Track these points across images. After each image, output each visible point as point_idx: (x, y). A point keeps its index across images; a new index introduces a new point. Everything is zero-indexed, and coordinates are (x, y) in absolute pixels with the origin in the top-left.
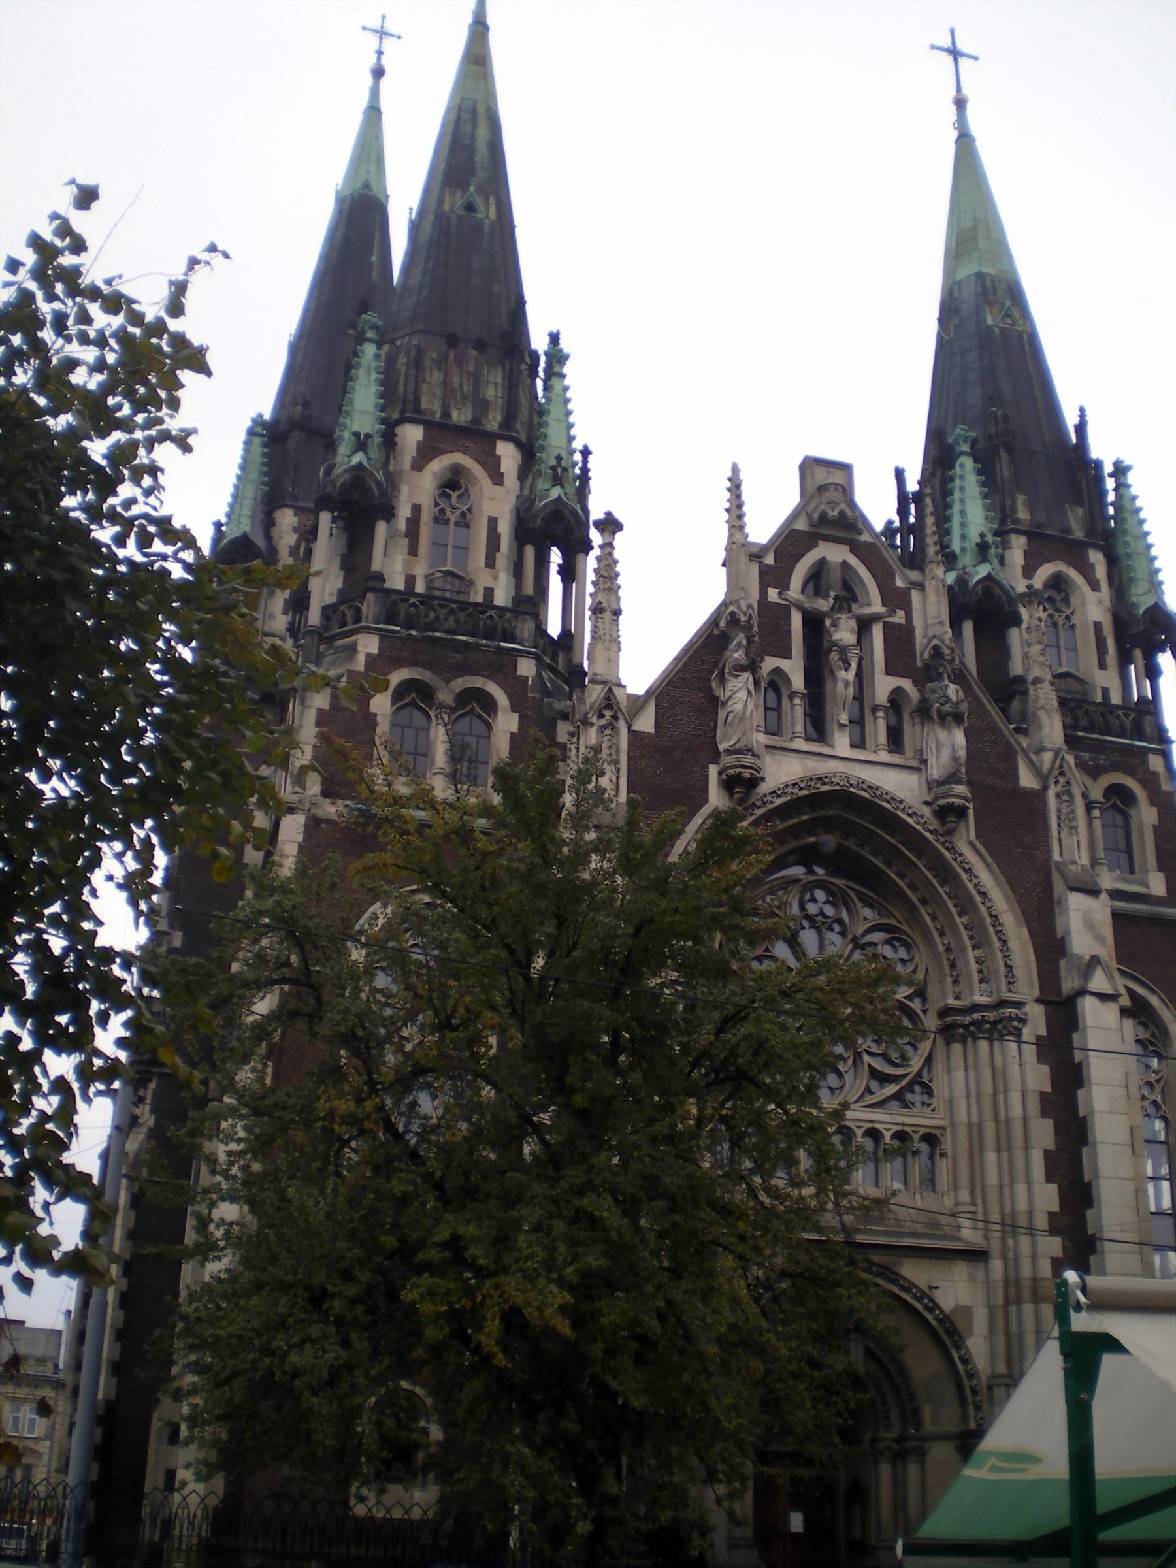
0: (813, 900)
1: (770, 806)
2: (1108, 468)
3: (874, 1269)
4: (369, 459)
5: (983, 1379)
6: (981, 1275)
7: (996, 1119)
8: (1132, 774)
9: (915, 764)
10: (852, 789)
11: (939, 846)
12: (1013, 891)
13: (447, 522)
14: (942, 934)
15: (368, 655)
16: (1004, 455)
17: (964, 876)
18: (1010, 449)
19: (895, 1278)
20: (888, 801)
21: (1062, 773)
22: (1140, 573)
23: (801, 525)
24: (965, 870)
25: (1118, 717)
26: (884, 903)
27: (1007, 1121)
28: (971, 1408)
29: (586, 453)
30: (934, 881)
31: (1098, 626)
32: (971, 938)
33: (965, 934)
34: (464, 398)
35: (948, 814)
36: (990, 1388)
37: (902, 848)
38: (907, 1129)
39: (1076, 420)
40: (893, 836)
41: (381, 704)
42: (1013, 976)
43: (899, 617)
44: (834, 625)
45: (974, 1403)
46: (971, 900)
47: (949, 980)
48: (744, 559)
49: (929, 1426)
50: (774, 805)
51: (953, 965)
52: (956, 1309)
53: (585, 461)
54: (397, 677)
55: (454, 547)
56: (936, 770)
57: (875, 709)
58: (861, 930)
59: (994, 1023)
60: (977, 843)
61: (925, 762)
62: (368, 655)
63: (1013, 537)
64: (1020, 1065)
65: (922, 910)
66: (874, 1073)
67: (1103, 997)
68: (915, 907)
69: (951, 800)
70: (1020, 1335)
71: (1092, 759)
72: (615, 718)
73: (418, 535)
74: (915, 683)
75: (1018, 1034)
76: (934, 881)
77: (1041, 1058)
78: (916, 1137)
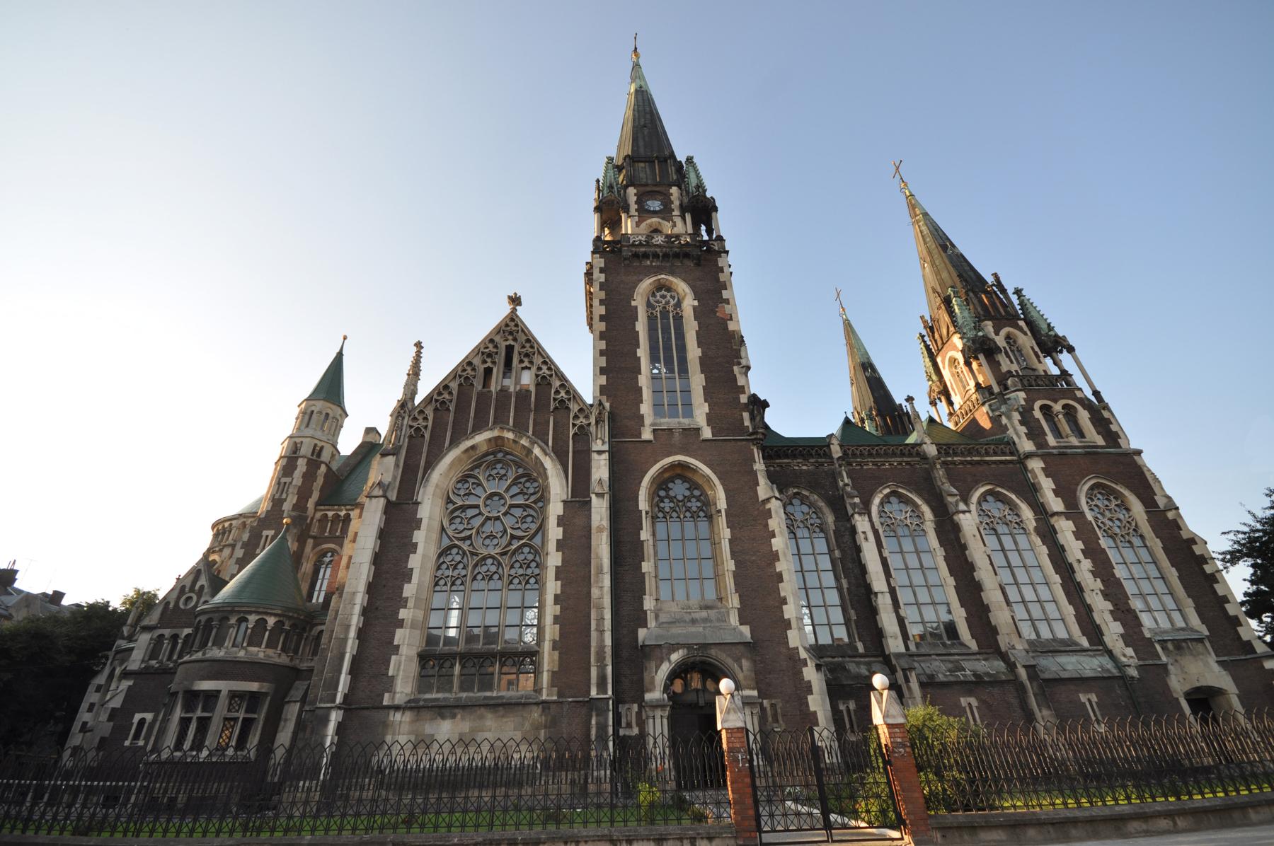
66: (513, 537)
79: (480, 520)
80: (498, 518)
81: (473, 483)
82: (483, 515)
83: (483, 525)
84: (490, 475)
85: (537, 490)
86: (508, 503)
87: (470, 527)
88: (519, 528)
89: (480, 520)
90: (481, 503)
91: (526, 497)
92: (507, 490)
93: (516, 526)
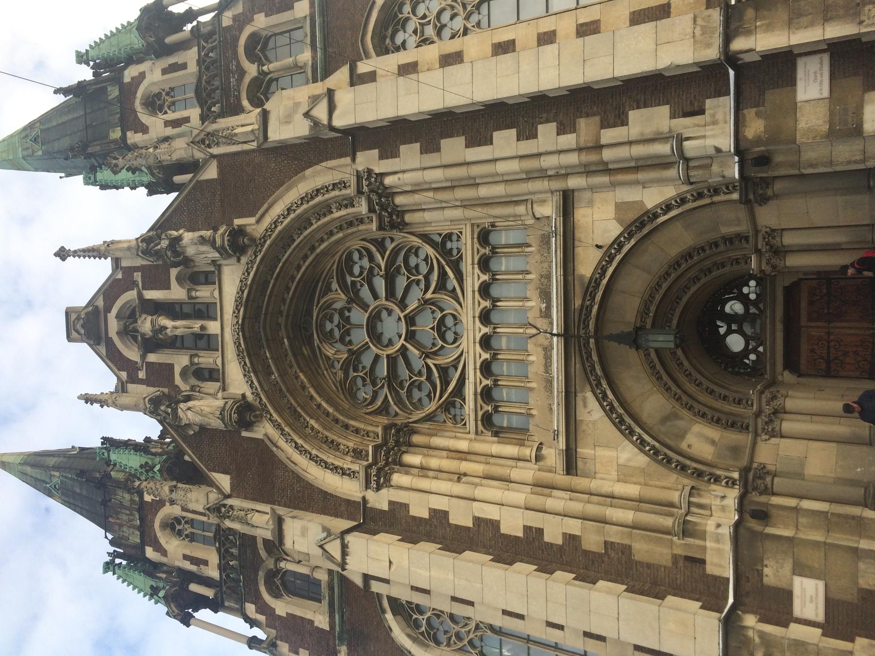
0: (332, 330)
1: (259, 390)
3: (588, 303)
4: (164, 588)
5: (686, 188)
6: (587, 195)
7: (452, 188)
8: (236, 39)
10: (240, 322)
11: (264, 249)
12: (283, 183)
13: (193, 533)
14: (331, 234)
17: (280, 228)
19: (594, 282)
20: (243, 292)
21: (203, 141)
23: (103, 349)
24: (276, 227)
25: (207, 55)
26: (325, 272)
27: (447, 180)
28: (716, 199)
30: (293, 247)
31: (165, 72)
32: (325, 215)
33: (324, 220)
34: (131, 514)
36: (691, 184)
37: (275, 274)
38: (476, 261)
40: (270, 282)
41: (282, 607)
42: (340, 183)
43: (138, 276)
45: (711, 196)
46: (299, 217)
47: (362, 227)
48: (124, 399)
49: (743, 227)
50: (258, 387)
51: (351, 224)
52: (619, 221)
55: (204, 531)
57: (190, 297)
58: (343, 296)
59: (380, 196)
60: (258, 216)
62: (257, 612)
63: (129, 142)
64: (404, 172)
65: (318, 251)
66: (442, 286)
67: (332, 108)
68: (318, 255)
69: (228, 248)
70: (637, 159)
71: (234, 77)
72: (224, 506)
73: (197, 559)
75: (382, 175)
76: (293, 247)
77: (395, 154)
78: (483, 251)
79: (413, 351)
80: (410, 320)
81: (355, 370)
82: (403, 350)
83: (418, 345)
84: (342, 340)
85: (365, 253)
86: (384, 302)
87: (425, 371)
88: (427, 278)
89: (413, 351)
90: (384, 354)
91: (376, 269)
92: (365, 306)
93: (422, 286)
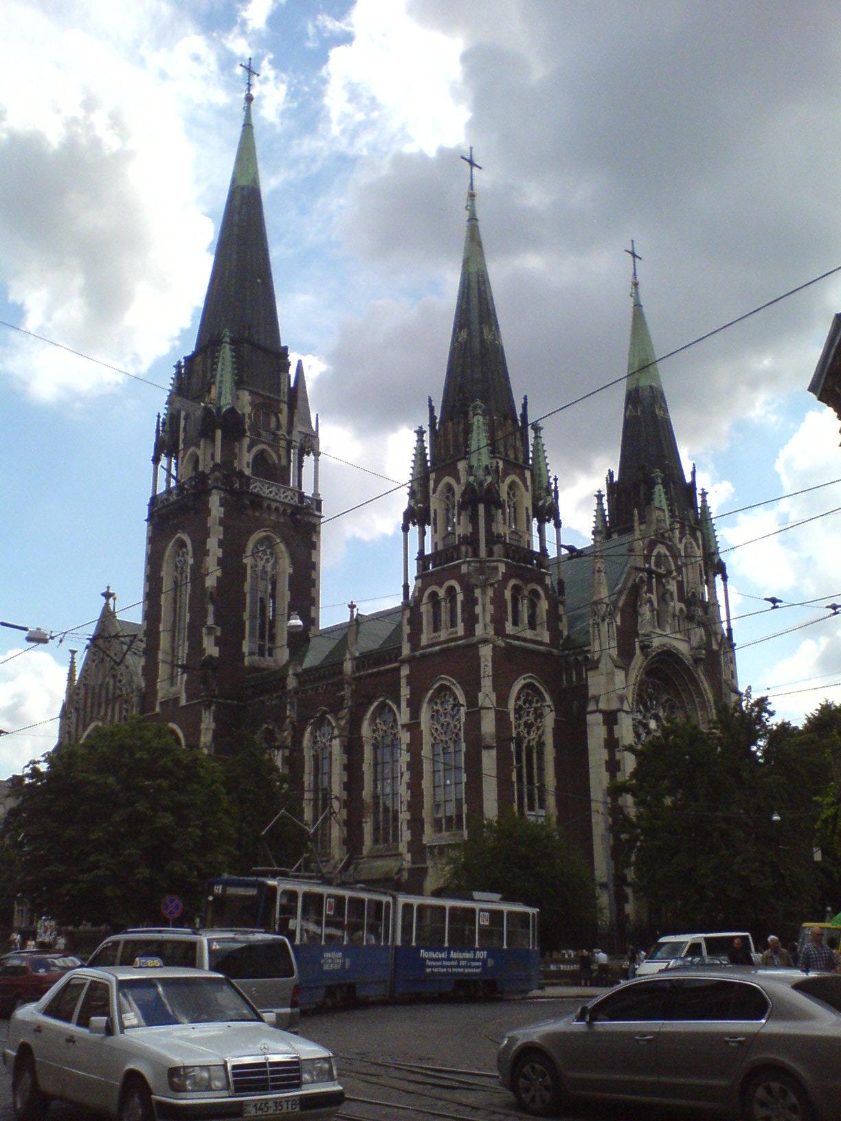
2: (699, 491)
9: (687, 639)
15: (502, 573)
16: (672, 485)
18: (674, 483)
22: (713, 544)
29: (556, 480)
35: (697, 661)
39: (691, 469)
41: (508, 594)
43: (680, 579)
44: (668, 582)
53: (556, 484)
54: (512, 582)
56: (694, 644)
61: (690, 639)
62: (502, 573)
68: (680, 694)
74: (686, 607)
